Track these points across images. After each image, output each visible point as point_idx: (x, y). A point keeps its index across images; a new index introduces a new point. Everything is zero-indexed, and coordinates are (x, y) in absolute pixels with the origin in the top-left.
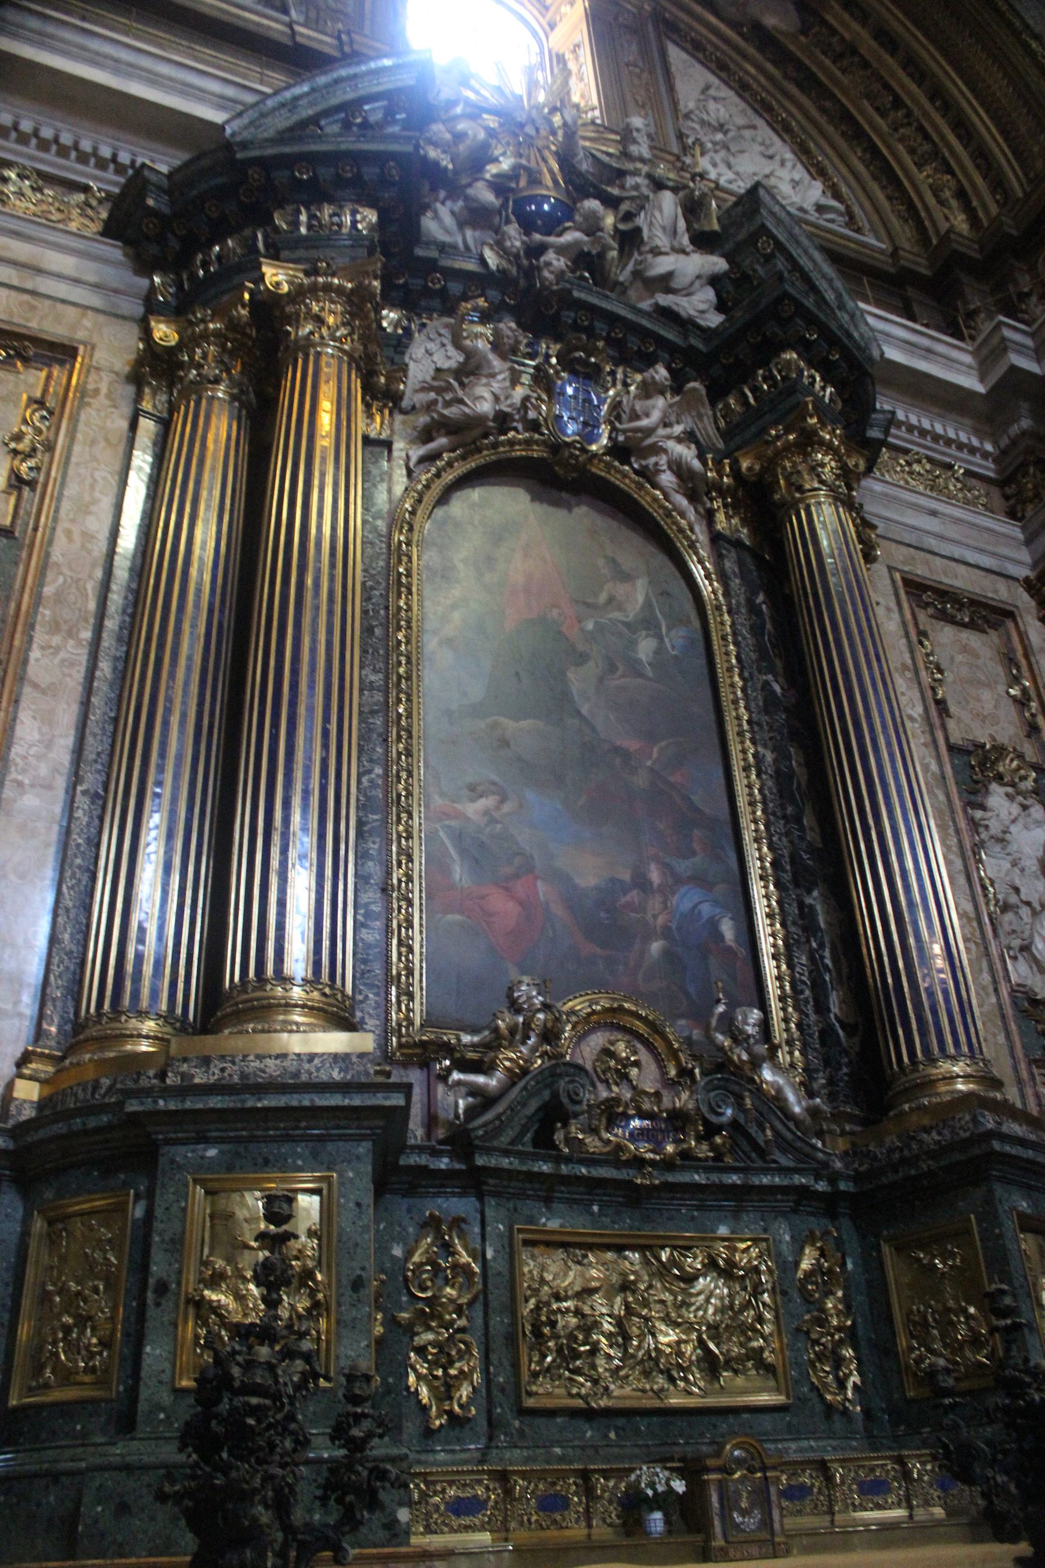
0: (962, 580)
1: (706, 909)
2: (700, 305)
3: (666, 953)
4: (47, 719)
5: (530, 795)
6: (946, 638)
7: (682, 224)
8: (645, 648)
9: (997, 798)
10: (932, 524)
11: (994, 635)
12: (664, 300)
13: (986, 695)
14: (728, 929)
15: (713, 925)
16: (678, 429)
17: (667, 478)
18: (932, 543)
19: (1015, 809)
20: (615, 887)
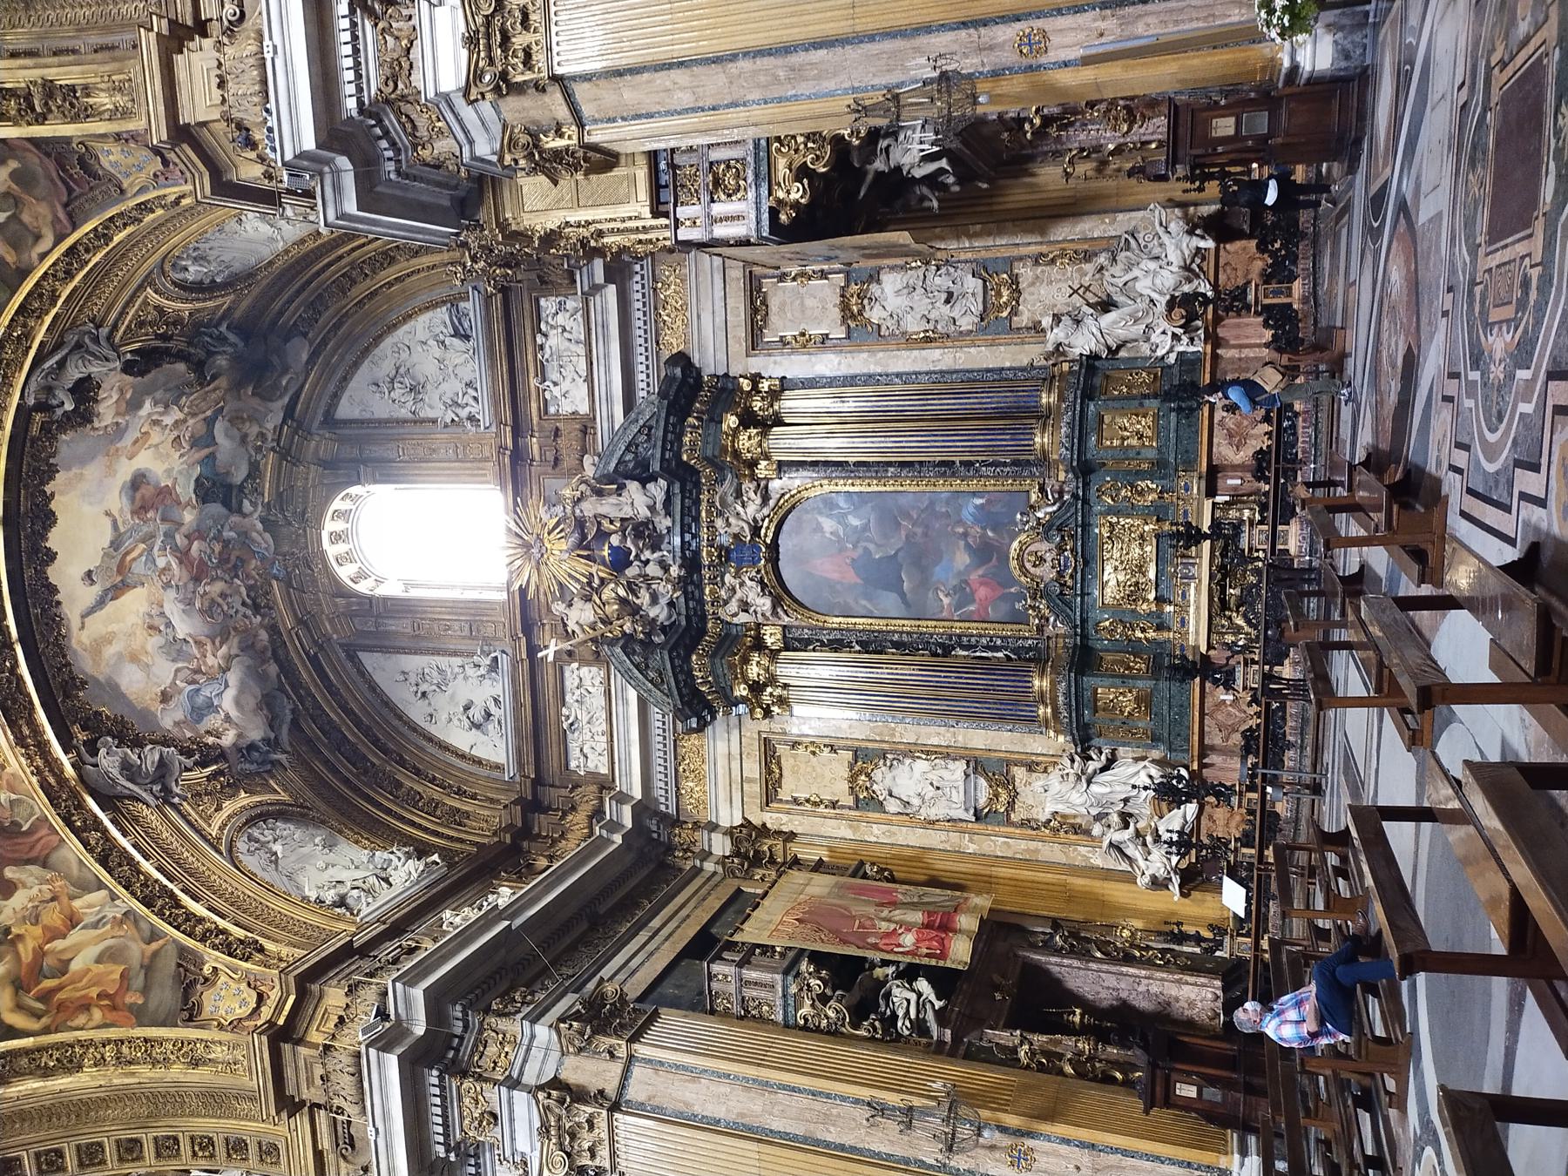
0: (738, 303)
1: (971, 509)
2: (658, 489)
3: (993, 530)
4: (929, 736)
5: (935, 579)
6: (780, 326)
7: (613, 500)
8: (855, 522)
9: (875, 315)
10: (706, 318)
11: (767, 283)
12: (659, 506)
13: (809, 302)
14: (979, 501)
15: (976, 507)
16: (739, 508)
17: (766, 511)
18: (720, 319)
19: (877, 307)
20: (968, 546)
